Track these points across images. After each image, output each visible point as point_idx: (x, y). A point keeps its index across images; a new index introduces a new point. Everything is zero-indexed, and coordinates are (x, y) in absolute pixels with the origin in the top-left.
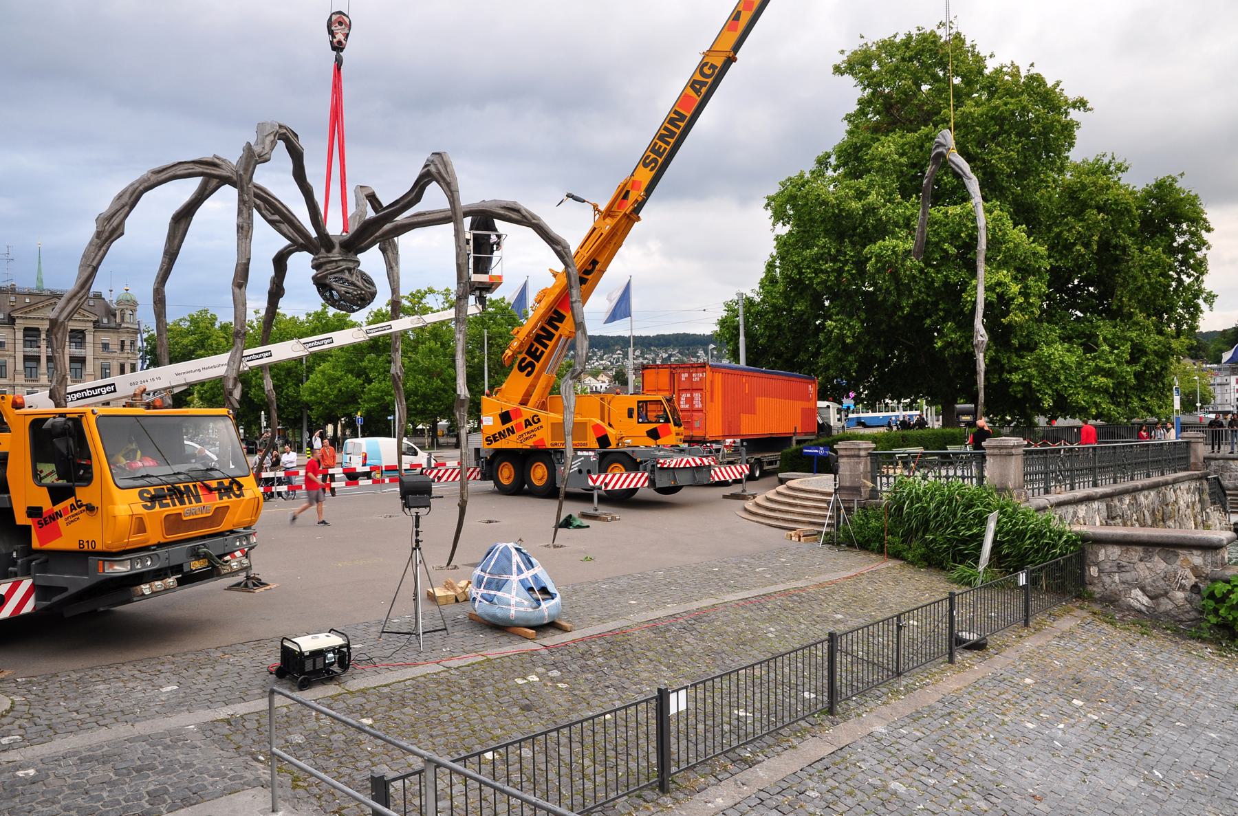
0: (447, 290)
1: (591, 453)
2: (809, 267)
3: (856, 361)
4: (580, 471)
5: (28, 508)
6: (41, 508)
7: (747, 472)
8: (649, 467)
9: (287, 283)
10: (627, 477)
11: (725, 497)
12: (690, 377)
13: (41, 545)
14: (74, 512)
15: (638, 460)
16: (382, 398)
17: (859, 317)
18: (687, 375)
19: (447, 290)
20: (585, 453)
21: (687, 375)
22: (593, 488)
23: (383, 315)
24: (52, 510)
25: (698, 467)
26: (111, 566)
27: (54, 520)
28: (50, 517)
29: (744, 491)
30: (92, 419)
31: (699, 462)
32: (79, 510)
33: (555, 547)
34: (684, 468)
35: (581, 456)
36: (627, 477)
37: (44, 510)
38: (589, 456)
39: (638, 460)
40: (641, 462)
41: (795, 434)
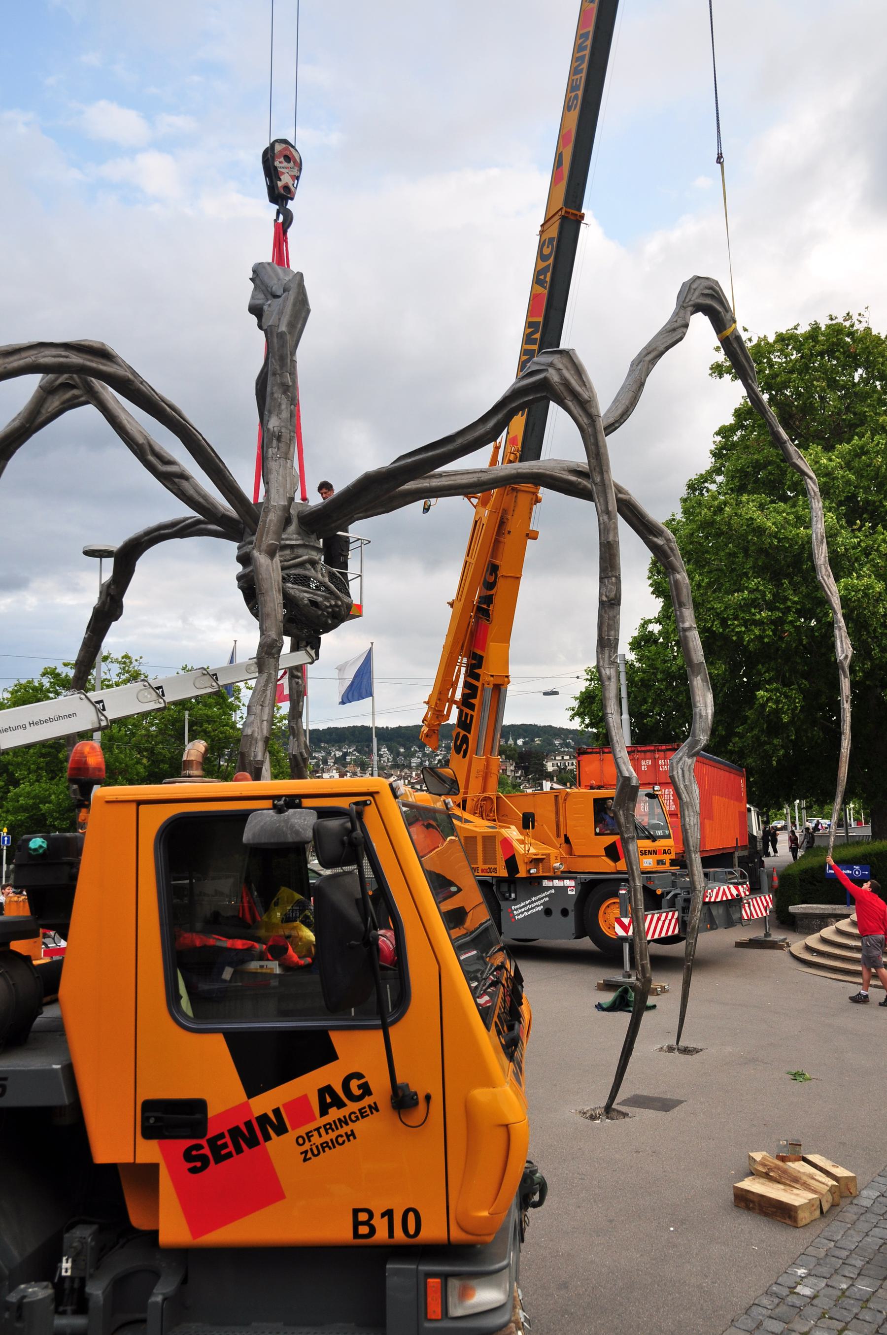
0: (126, 657)
1: (567, 883)
2: (736, 618)
3: (782, 747)
4: (548, 912)
5: (149, 1106)
6: (198, 1106)
7: (771, 906)
8: (679, 902)
9: (128, 600)
10: (659, 919)
11: (739, 945)
12: (655, 765)
13: (196, 1230)
14: (334, 1114)
15: (659, 892)
16: (35, 806)
17: (799, 686)
18: (649, 762)
19: (126, 657)
20: (557, 883)
21: (649, 762)
22: (623, 939)
23: (35, 689)
24: (245, 1106)
25: (733, 899)
26: (464, 1294)
27: (253, 1142)
28: (235, 1132)
29: (767, 935)
30: (395, 813)
31: (735, 893)
32: (353, 1107)
33: (686, 1051)
34: (722, 901)
35: (549, 888)
36: (659, 919)
37: (211, 1112)
38: (566, 888)
39: (659, 892)
40: (662, 895)
41: (736, 848)
